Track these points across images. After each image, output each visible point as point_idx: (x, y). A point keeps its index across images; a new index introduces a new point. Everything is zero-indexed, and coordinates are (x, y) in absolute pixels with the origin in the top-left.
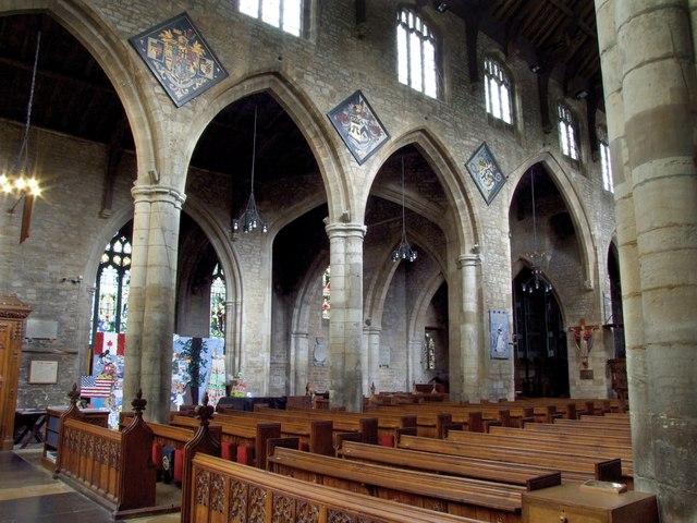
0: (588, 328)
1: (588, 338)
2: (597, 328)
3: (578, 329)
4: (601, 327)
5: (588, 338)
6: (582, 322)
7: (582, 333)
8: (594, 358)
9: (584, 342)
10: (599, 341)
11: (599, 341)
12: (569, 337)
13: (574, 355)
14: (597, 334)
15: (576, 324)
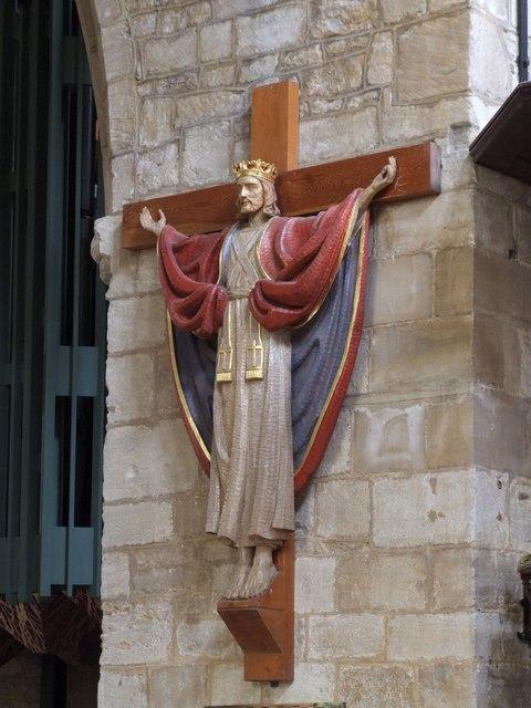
0: (305, 191)
1: (301, 304)
2: (402, 182)
3: (219, 209)
4: (451, 164)
5: (301, 304)
6: (264, 122)
7: (247, 254)
8: (354, 550)
9: (256, 364)
10: (425, 340)
11: (425, 340)
12: (131, 314)
13: (160, 525)
14: (411, 265)
15: (202, 161)
